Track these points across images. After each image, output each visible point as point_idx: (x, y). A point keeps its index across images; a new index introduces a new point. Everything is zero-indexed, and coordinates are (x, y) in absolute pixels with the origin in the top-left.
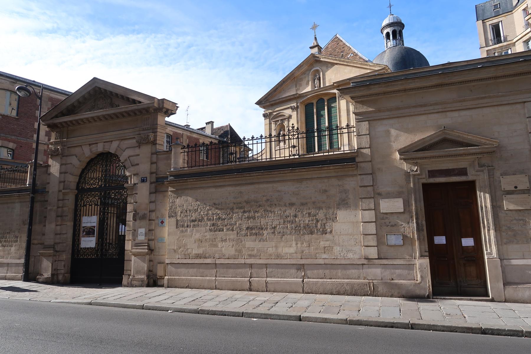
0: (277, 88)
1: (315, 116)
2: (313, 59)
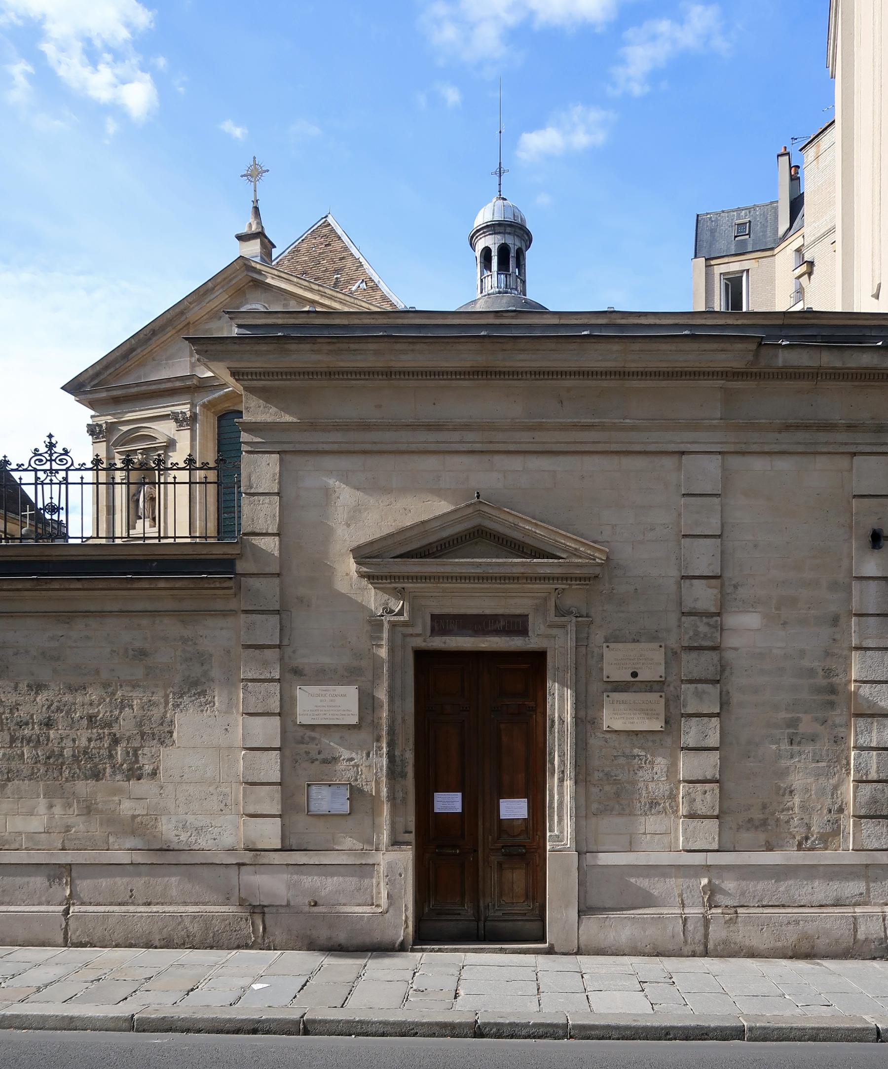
0: (132, 350)
2: (245, 273)
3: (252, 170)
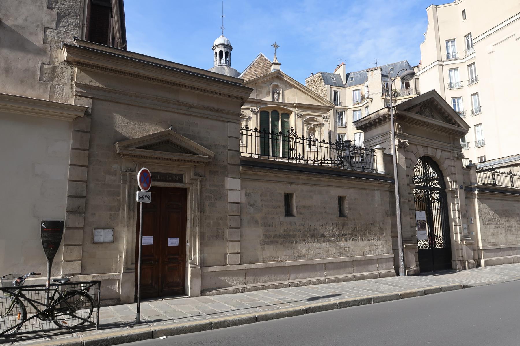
1: (270, 125)
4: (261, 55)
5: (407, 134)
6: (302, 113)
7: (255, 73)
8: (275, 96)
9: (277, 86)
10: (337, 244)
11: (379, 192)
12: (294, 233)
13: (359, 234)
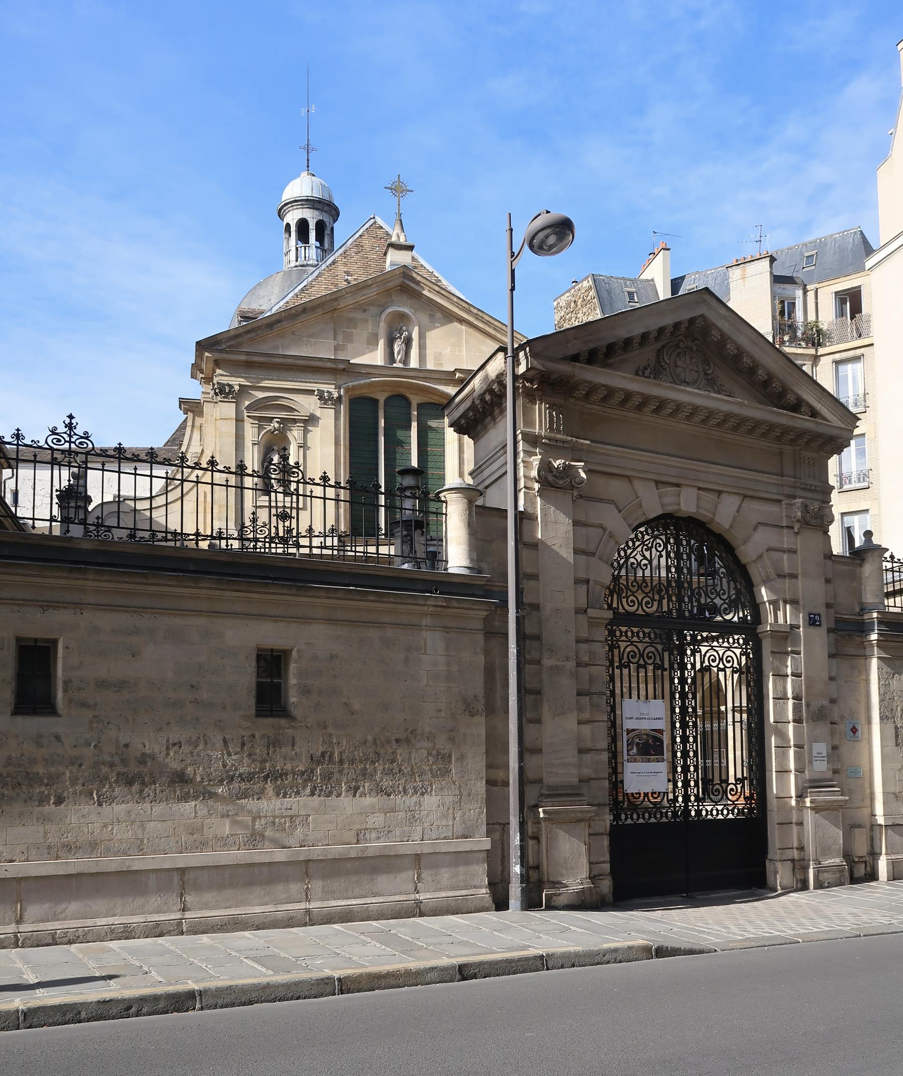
0: (279, 321)
3: (396, 186)
4: (375, 222)
5: (588, 442)
6: (236, 382)
7: (346, 280)
8: (396, 349)
9: (403, 317)
10: (243, 807)
11: (438, 634)
12: (52, 770)
13: (340, 772)
